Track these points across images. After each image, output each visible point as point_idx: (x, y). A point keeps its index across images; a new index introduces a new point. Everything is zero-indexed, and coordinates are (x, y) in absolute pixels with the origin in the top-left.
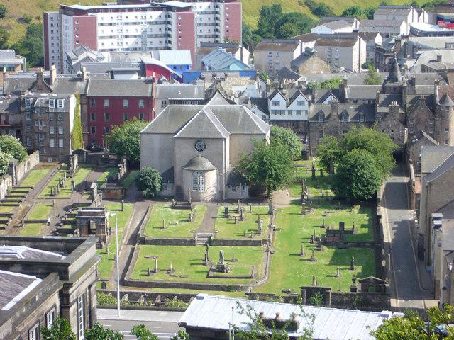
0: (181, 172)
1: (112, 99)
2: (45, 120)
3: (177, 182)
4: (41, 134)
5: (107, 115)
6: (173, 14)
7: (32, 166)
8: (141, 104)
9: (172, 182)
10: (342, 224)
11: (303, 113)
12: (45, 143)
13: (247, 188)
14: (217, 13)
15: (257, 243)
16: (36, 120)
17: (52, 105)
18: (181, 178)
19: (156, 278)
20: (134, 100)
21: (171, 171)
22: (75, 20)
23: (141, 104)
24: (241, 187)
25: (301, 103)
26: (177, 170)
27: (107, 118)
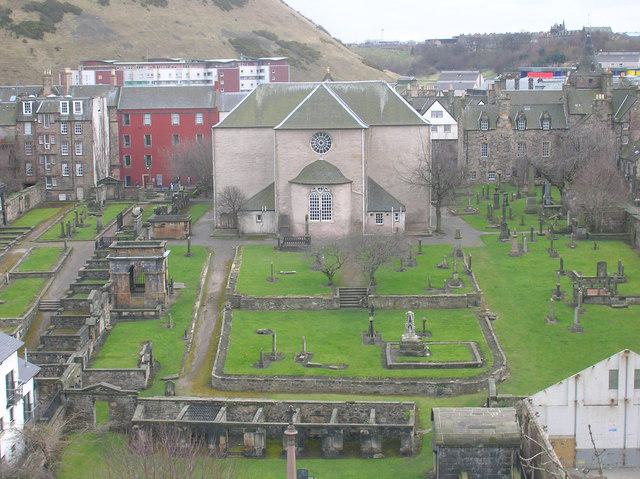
0: (288, 191)
1: (154, 113)
2: (54, 134)
3: (281, 208)
4: (48, 156)
5: (148, 137)
6: (214, 71)
7: (33, 203)
8: (199, 120)
9: (272, 210)
10: (601, 265)
11: (441, 130)
12: (54, 170)
13: (402, 217)
14: (260, 78)
15: (454, 305)
16: (40, 134)
17: (65, 110)
18: (288, 201)
19: (277, 369)
20: (187, 115)
21: (270, 189)
22: (97, 74)
23: (199, 120)
24: (393, 215)
25: (437, 114)
26: (281, 186)
27: (148, 143)
